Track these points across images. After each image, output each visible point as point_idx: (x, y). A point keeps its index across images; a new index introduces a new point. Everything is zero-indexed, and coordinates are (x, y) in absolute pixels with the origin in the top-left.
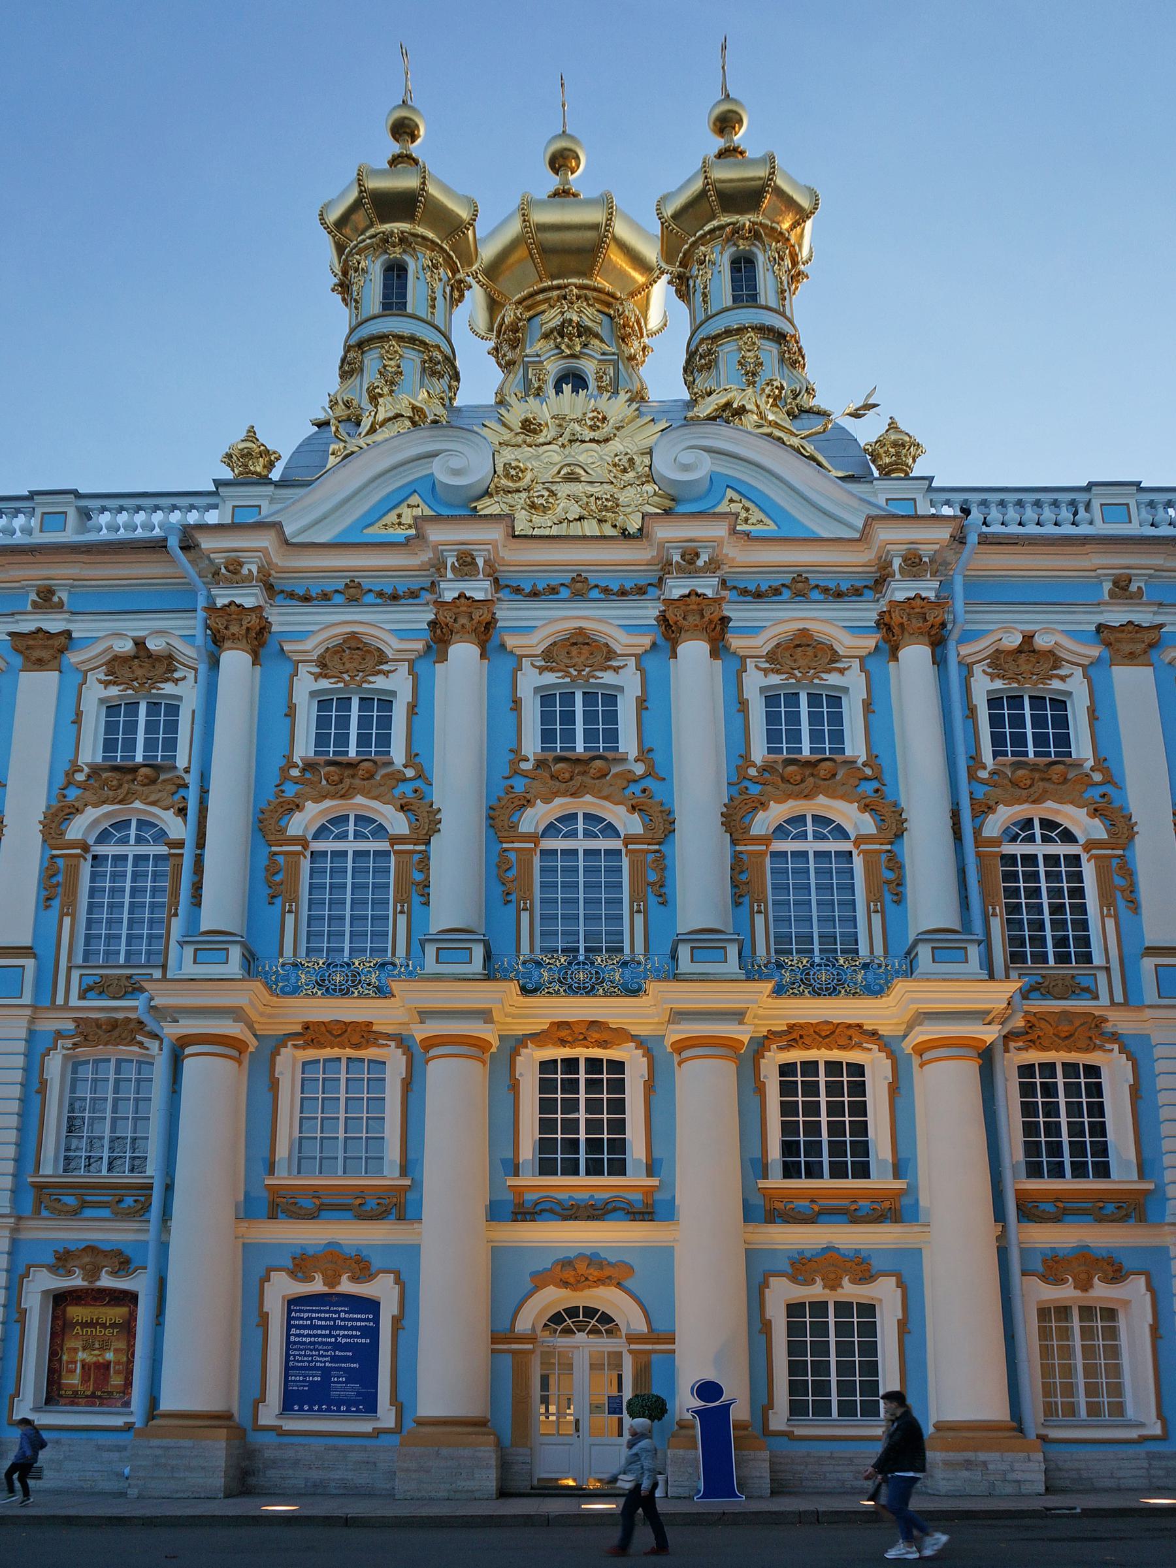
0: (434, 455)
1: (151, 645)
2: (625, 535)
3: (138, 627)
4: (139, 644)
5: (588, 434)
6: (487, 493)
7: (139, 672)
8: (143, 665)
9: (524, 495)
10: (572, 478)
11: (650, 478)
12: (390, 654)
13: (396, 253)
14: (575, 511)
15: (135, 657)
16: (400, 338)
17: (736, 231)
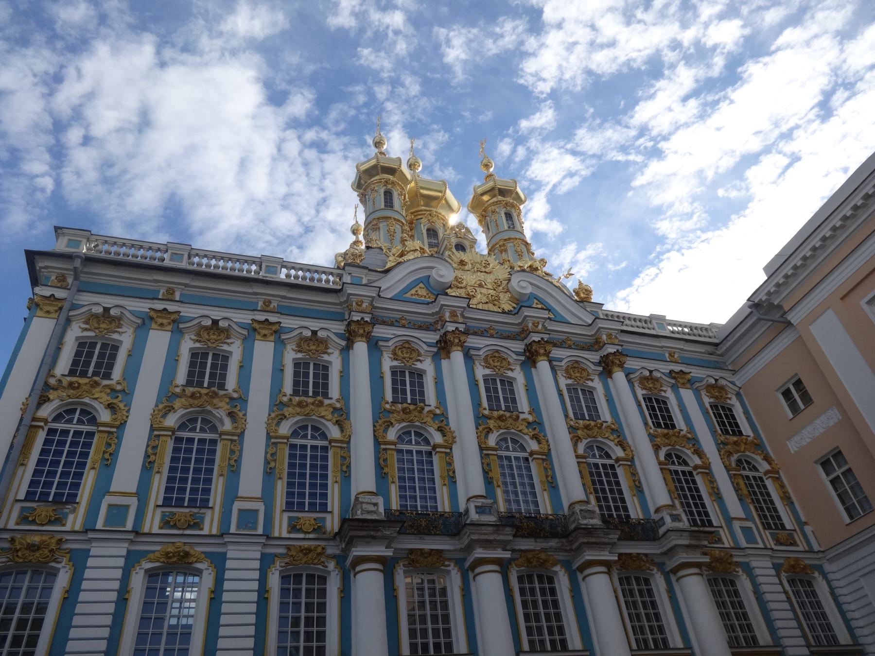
0: (432, 268)
1: (320, 334)
2: (504, 312)
3: (314, 325)
4: (314, 333)
5: (483, 270)
6: (450, 287)
7: (313, 347)
8: (314, 342)
9: (463, 290)
10: (481, 286)
11: (508, 291)
12: (422, 352)
13: (389, 186)
14: (485, 299)
15: (311, 340)
16: (395, 219)
17: (506, 204)
